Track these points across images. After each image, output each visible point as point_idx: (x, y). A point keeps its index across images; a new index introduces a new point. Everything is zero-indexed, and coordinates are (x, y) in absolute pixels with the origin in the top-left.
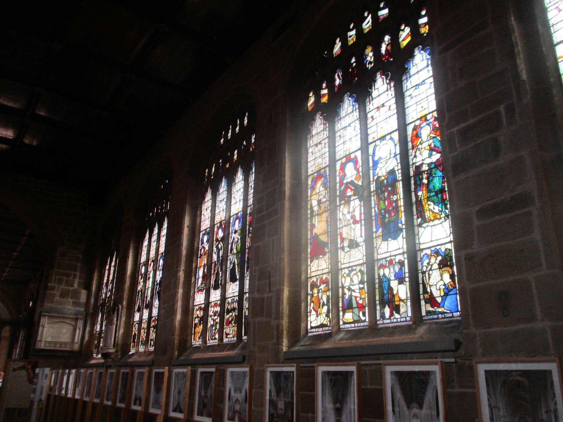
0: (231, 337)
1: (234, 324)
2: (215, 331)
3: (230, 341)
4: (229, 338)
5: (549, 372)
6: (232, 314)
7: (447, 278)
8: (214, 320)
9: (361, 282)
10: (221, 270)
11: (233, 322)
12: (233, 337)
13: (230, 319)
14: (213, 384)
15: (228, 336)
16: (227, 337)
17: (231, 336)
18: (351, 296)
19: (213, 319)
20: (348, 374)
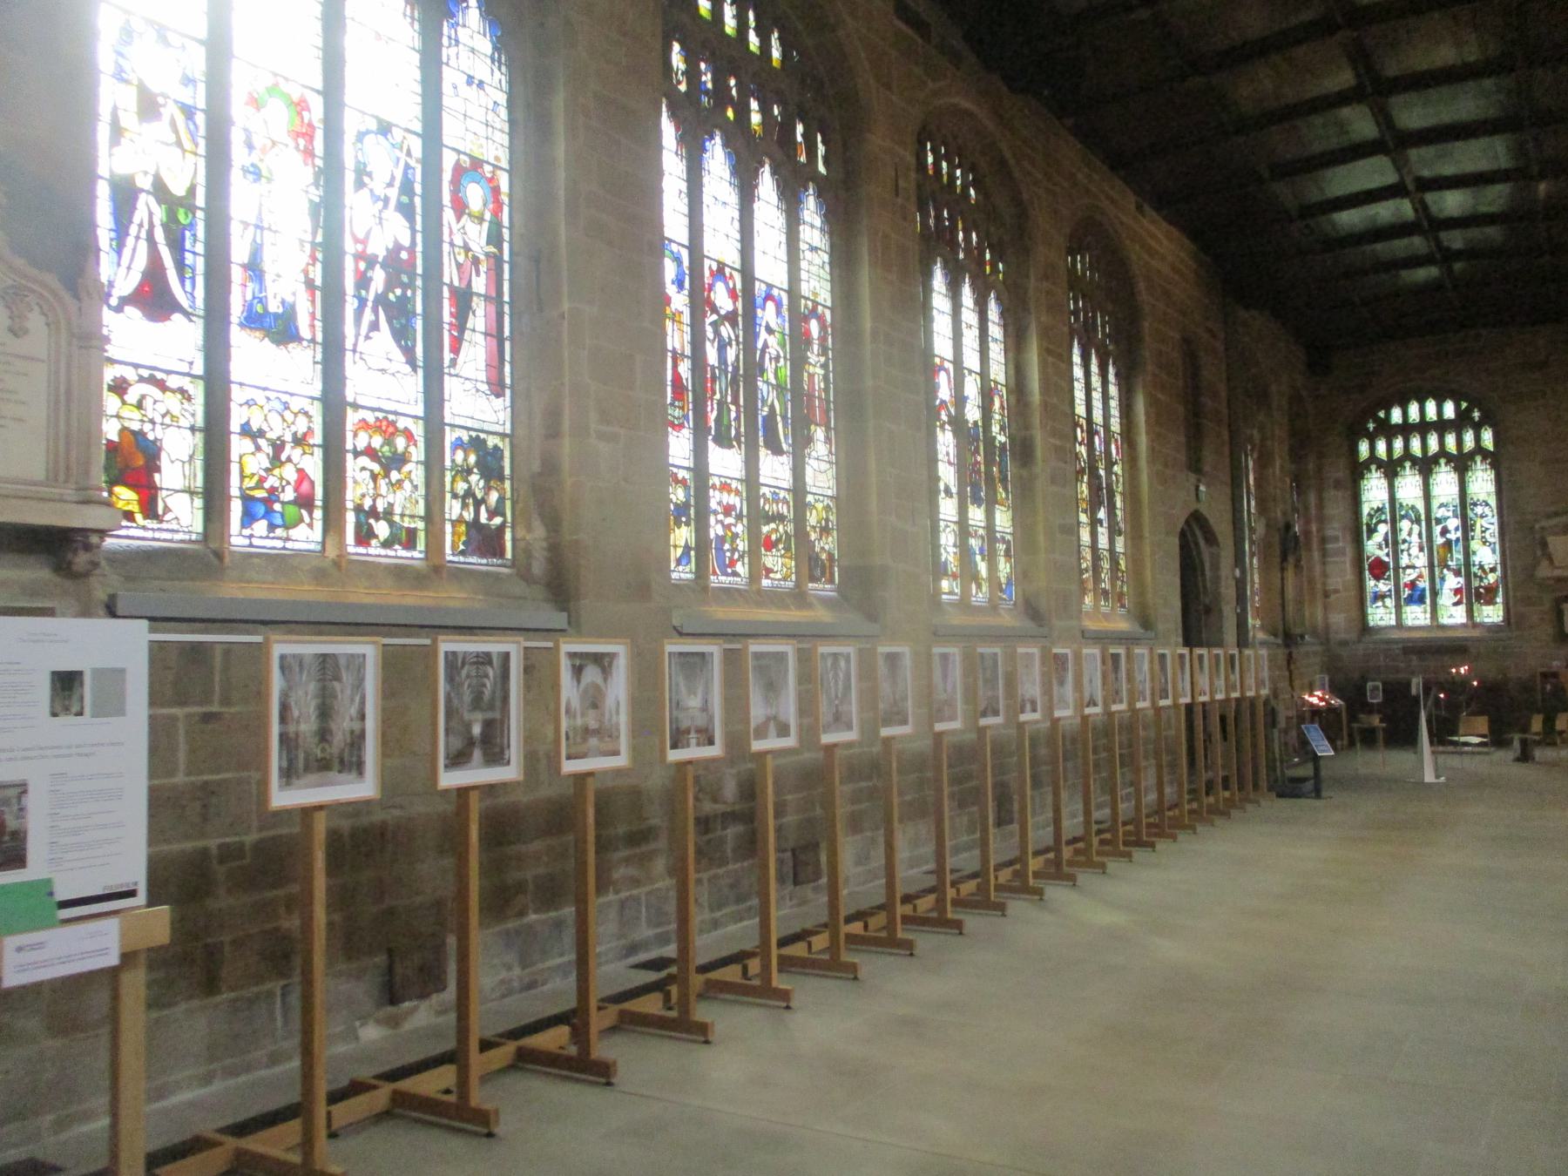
0: (779, 580)
1: (783, 552)
2: (733, 554)
3: (777, 587)
4: (772, 579)
5: (786, 653)
6: (778, 526)
7: (1008, 565)
8: (727, 527)
9: (955, 546)
10: (735, 401)
11: (781, 546)
12: (785, 579)
13: (774, 537)
14: (841, 675)
15: (772, 575)
16: (767, 577)
17: (778, 576)
18: (946, 559)
19: (722, 522)
20: (780, 657)
